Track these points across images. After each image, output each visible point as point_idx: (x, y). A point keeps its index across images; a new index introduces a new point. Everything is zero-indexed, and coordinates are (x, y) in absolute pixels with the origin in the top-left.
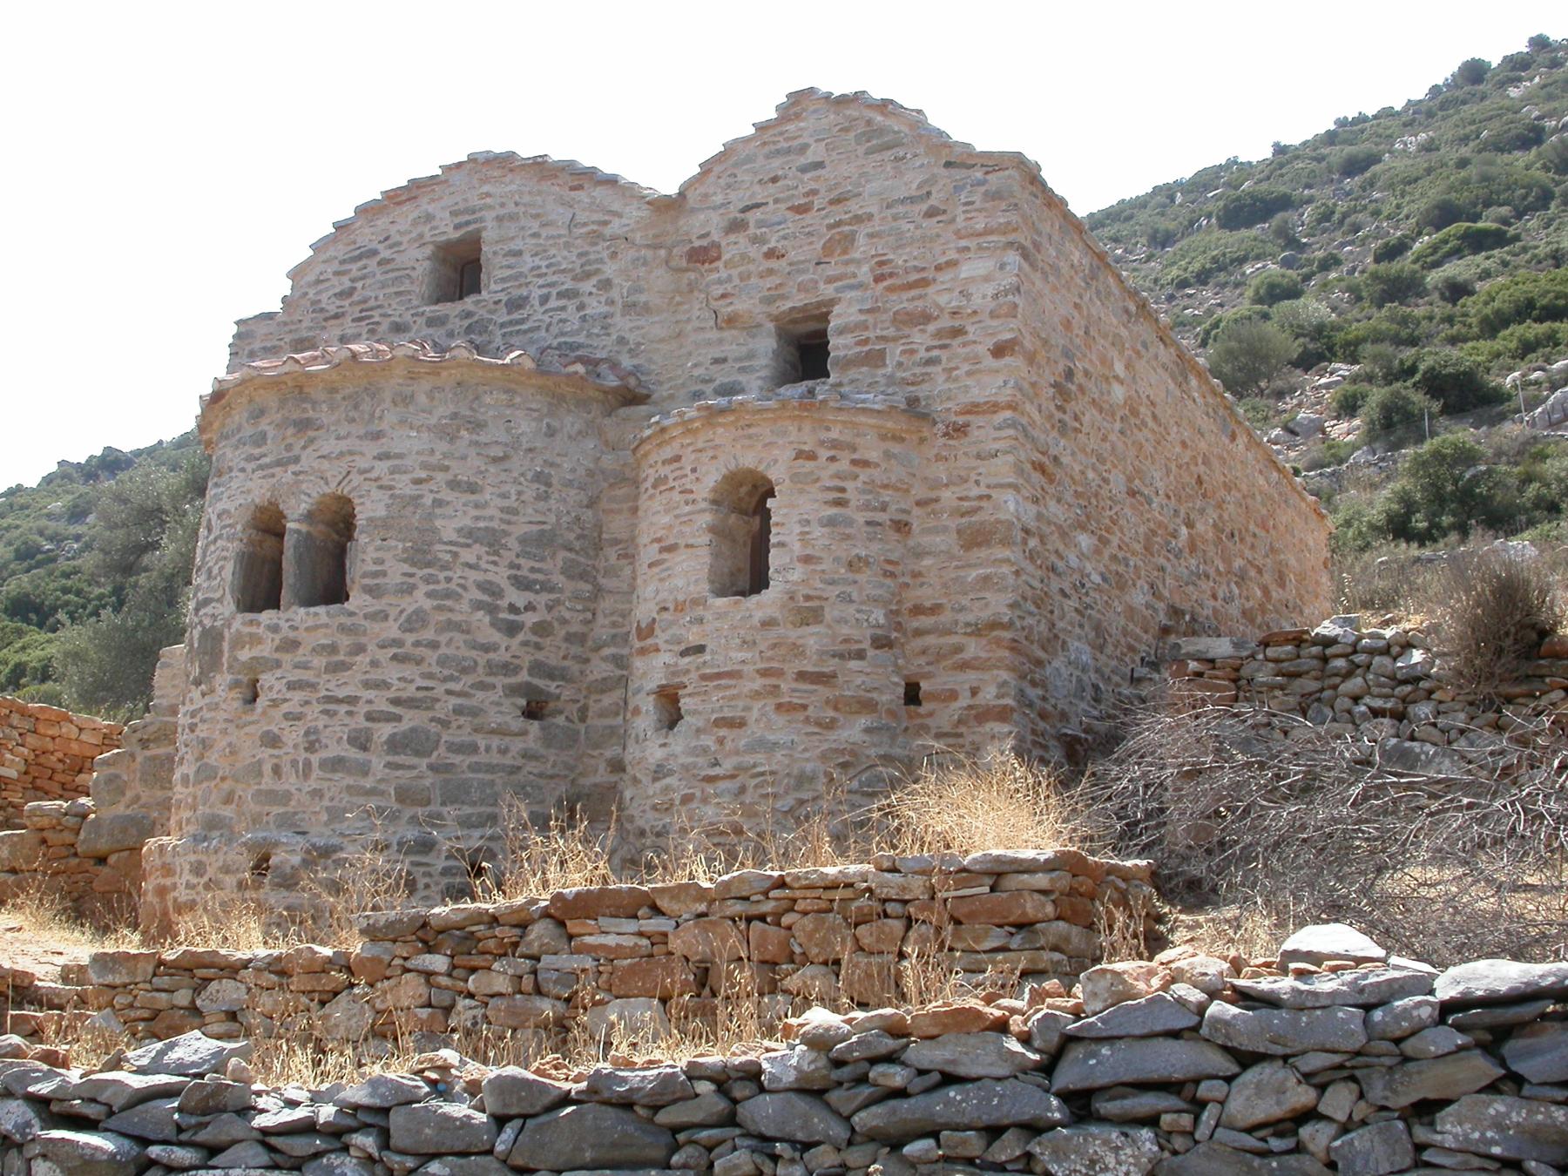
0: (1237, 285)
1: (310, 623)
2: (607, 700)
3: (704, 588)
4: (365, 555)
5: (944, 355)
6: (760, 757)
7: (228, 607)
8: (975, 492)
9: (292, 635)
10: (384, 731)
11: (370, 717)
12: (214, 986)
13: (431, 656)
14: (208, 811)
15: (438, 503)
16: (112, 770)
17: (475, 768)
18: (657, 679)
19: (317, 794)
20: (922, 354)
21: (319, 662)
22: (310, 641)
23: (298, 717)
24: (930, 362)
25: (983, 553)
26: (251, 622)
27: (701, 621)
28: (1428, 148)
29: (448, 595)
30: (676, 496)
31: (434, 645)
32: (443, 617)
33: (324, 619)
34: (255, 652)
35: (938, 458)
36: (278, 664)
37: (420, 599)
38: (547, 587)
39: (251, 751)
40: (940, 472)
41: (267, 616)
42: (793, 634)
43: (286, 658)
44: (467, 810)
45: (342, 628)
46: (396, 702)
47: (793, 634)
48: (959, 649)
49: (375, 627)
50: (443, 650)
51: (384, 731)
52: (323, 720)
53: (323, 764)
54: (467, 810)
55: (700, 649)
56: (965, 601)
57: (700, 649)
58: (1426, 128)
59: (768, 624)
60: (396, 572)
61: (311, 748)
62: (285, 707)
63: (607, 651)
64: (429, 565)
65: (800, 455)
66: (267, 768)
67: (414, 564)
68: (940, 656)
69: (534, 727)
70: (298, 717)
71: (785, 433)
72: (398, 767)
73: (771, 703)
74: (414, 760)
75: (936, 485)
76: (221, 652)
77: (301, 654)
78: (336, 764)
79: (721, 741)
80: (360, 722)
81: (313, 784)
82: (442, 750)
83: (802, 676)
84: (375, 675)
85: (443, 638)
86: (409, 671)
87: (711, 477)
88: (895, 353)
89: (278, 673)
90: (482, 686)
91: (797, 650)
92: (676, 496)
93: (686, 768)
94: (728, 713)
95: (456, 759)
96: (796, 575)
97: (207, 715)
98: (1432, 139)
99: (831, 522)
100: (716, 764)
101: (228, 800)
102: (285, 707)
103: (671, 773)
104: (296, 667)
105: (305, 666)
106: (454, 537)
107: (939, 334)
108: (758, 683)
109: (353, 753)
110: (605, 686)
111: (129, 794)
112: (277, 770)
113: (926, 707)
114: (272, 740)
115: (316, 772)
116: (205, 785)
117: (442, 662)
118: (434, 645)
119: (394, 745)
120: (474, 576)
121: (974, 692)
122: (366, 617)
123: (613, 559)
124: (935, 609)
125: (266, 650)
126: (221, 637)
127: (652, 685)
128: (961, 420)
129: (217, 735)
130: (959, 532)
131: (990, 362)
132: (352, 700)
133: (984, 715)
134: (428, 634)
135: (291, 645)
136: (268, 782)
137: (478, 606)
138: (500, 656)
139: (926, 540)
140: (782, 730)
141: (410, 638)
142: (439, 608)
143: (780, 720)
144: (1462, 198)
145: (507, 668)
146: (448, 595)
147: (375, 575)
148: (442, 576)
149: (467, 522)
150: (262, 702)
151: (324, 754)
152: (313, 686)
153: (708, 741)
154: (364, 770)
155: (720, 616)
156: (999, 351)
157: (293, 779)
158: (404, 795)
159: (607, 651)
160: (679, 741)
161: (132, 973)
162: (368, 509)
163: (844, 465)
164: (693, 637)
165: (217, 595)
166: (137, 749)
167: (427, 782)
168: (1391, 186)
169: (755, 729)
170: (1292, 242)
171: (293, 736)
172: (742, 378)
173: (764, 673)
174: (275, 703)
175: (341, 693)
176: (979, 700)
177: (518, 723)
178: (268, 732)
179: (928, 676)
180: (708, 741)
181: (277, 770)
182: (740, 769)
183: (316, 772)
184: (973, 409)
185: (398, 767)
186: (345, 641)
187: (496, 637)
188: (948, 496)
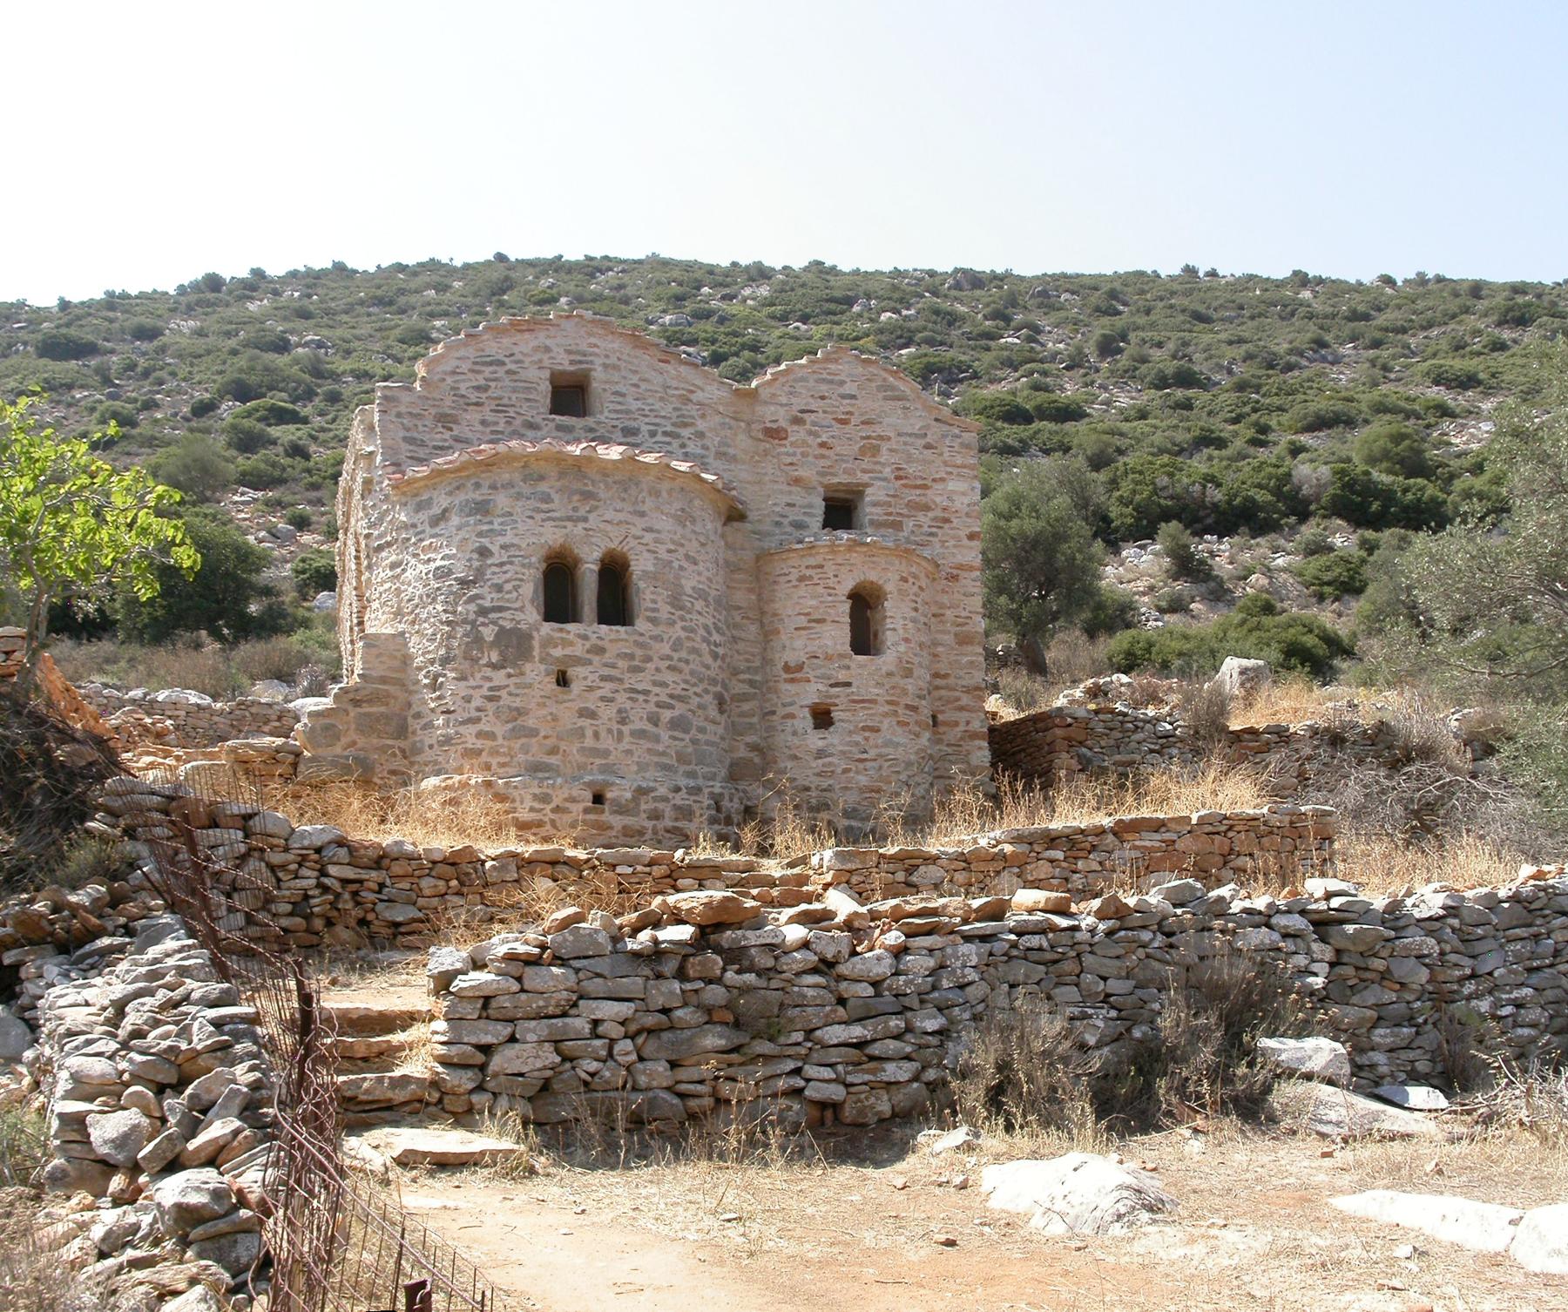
0: (70, 405)
1: (613, 636)
2: (746, 707)
3: (848, 648)
4: (646, 595)
5: (940, 532)
6: (890, 750)
7: (531, 616)
8: (964, 614)
9: (600, 643)
10: (667, 715)
11: (658, 705)
12: (922, 869)
13: (686, 669)
14: (530, 758)
15: (681, 568)
16: (327, 721)
17: (708, 743)
18: (813, 699)
19: (629, 752)
20: (926, 529)
21: (622, 664)
22: (612, 651)
23: (612, 700)
24: (931, 534)
25: (970, 648)
26: (561, 630)
27: (848, 668)
28: (200, 333)
29: (693, 631)
30: (820, 589)
31: (687, 662)
32: (690, 644)
33: (624, 636)
34: (568, 651)
35: (943, 591)
36: (590, 663)
37: (678, 632)
38: (723, 634)
39: (569, 719)
40: (945, 599)
41: (571, 627)
42: (902, 682)
43: (596, 659)
44: (706, 769)
45: (636, 643)
46: (671, 696)
47: (902, 682)
48: (958, 699)
49: (657, 646)
50: (692, 666)
51: (667, 715)
52: (628, 705)
53: (633, 733)
54: (706, 769)
55: (848, 684)
56: (961, 673)
57: (848, 684)
58: (194, 318)
59: (890, 674)
60: (665, 611)
61: (623, 721)
62: (600, 693)
63: (742, 676)
64: (681, 608)
65: (904, 580)
66: (589, 733)
67: (673, 606)
68: (948, 702)
69: (722, 719)
70: (612, 700)
71: (892, 564)
72: (675, 738)
73: (894, 720)
74: (681, 735)
75: (942, 606)
76: (531, 648)
77: (608, 657)
78: (640, 734)
79: (866, 739)
80: (651, 707)
81: (625, 745)
82: (693, 731)
83: (908, 707)
84: (658, 677)
85: (691, 657)
86: (676, 677)
87: (848, 585)
88: (909, 524)
89: (590, 668)
90: (706, 691)
91: (905, 692)
92: (820, 589)
93: (843, 753)
94: (870, 723)
95: (700, 736)
96: (902, 648)
97: (512, 688)
98: (202, 328)
99: (914, 621)
100: (865, 752)
101: (553, 751)
102: (600, 693)
103: (831, 755)
104: (606, 665)
105: (613, 666)
106: (690, 592)
107: (935, 519)
108: (887, 708)
109: (649, 727)
110: (744, 698)
111: (344, 741)
112: (596, 735)
113: (942, 729)
114: (592, 715)
115: (627, 739)
116: (524, 740)
117: (692, 673)
118: (687, 662)
119: (675, 724)
120: (702, 620)
121: (968, 723)
122: (651, 638)
123: (738, 619)
124: (946, 676)
125: (579, 650)
126: (531, 637)
127: (809, 702)
128: (955, 572)
129: (533, 706)
130: (956, 635)
131: (965, 542)
132: (646, 692)
133: (974, 736)
134: (684, 654)
135: (600, 650)
136: (589, 742)
137: (705, 640)
138: (712, 673)
139: (939, 636)
140: (901, 737)
141: (676, 656)
142: (688, 638)
143: (899, 730)
144: (253, 379)
145: (713, 682)
146: (693, 631)
147: (654, 610)
148: (688, 617)
149: (694, 583)
150: (576, 687)
151: (631, 726)
152: (620, 680)
153: (858, 738)
154: (657, 739)
155: (861, 666)
156: (971, 537)
157: (610, 741)
158: (682, 758)
159: (742, 676)
160: (833, 739)
161: (863, 862)
162: (640, 565)
163: (915, 589)
164: (842, 676)
165: (517, 605)
166: (350, 708)
167: (690, 750)
168: (180, 357)
169: (886, 734)
170: (107, 381)
171: (607, 713)
172: (806, 519)
173: (888, 702)
174: (590, 689)
175: (640, 687)
176: (970, 728)
177: (718, 717)
178: (586, 709)
179: (942, 712)
180: (858, 738)
181: (596, 735)
182: (881, 756)
183: (627, 739)
184: (960, 567)
185: (675, 738)
186: (639, 652)
187: (709, 660)
188: (948, 612)
